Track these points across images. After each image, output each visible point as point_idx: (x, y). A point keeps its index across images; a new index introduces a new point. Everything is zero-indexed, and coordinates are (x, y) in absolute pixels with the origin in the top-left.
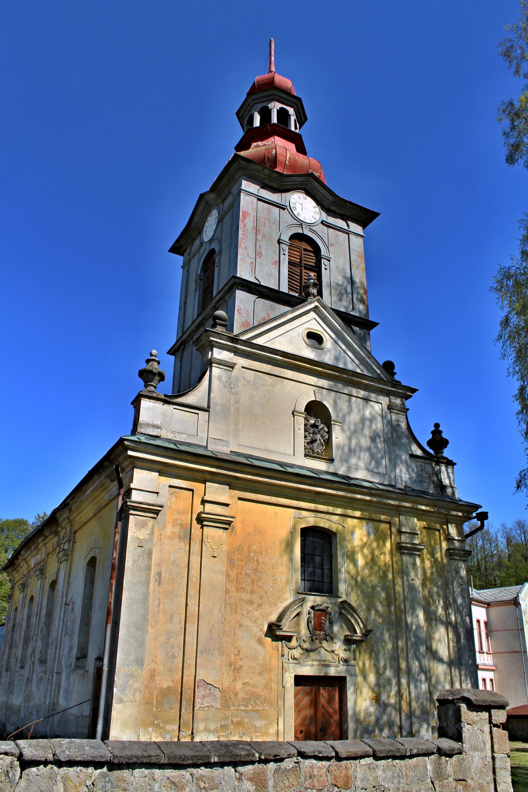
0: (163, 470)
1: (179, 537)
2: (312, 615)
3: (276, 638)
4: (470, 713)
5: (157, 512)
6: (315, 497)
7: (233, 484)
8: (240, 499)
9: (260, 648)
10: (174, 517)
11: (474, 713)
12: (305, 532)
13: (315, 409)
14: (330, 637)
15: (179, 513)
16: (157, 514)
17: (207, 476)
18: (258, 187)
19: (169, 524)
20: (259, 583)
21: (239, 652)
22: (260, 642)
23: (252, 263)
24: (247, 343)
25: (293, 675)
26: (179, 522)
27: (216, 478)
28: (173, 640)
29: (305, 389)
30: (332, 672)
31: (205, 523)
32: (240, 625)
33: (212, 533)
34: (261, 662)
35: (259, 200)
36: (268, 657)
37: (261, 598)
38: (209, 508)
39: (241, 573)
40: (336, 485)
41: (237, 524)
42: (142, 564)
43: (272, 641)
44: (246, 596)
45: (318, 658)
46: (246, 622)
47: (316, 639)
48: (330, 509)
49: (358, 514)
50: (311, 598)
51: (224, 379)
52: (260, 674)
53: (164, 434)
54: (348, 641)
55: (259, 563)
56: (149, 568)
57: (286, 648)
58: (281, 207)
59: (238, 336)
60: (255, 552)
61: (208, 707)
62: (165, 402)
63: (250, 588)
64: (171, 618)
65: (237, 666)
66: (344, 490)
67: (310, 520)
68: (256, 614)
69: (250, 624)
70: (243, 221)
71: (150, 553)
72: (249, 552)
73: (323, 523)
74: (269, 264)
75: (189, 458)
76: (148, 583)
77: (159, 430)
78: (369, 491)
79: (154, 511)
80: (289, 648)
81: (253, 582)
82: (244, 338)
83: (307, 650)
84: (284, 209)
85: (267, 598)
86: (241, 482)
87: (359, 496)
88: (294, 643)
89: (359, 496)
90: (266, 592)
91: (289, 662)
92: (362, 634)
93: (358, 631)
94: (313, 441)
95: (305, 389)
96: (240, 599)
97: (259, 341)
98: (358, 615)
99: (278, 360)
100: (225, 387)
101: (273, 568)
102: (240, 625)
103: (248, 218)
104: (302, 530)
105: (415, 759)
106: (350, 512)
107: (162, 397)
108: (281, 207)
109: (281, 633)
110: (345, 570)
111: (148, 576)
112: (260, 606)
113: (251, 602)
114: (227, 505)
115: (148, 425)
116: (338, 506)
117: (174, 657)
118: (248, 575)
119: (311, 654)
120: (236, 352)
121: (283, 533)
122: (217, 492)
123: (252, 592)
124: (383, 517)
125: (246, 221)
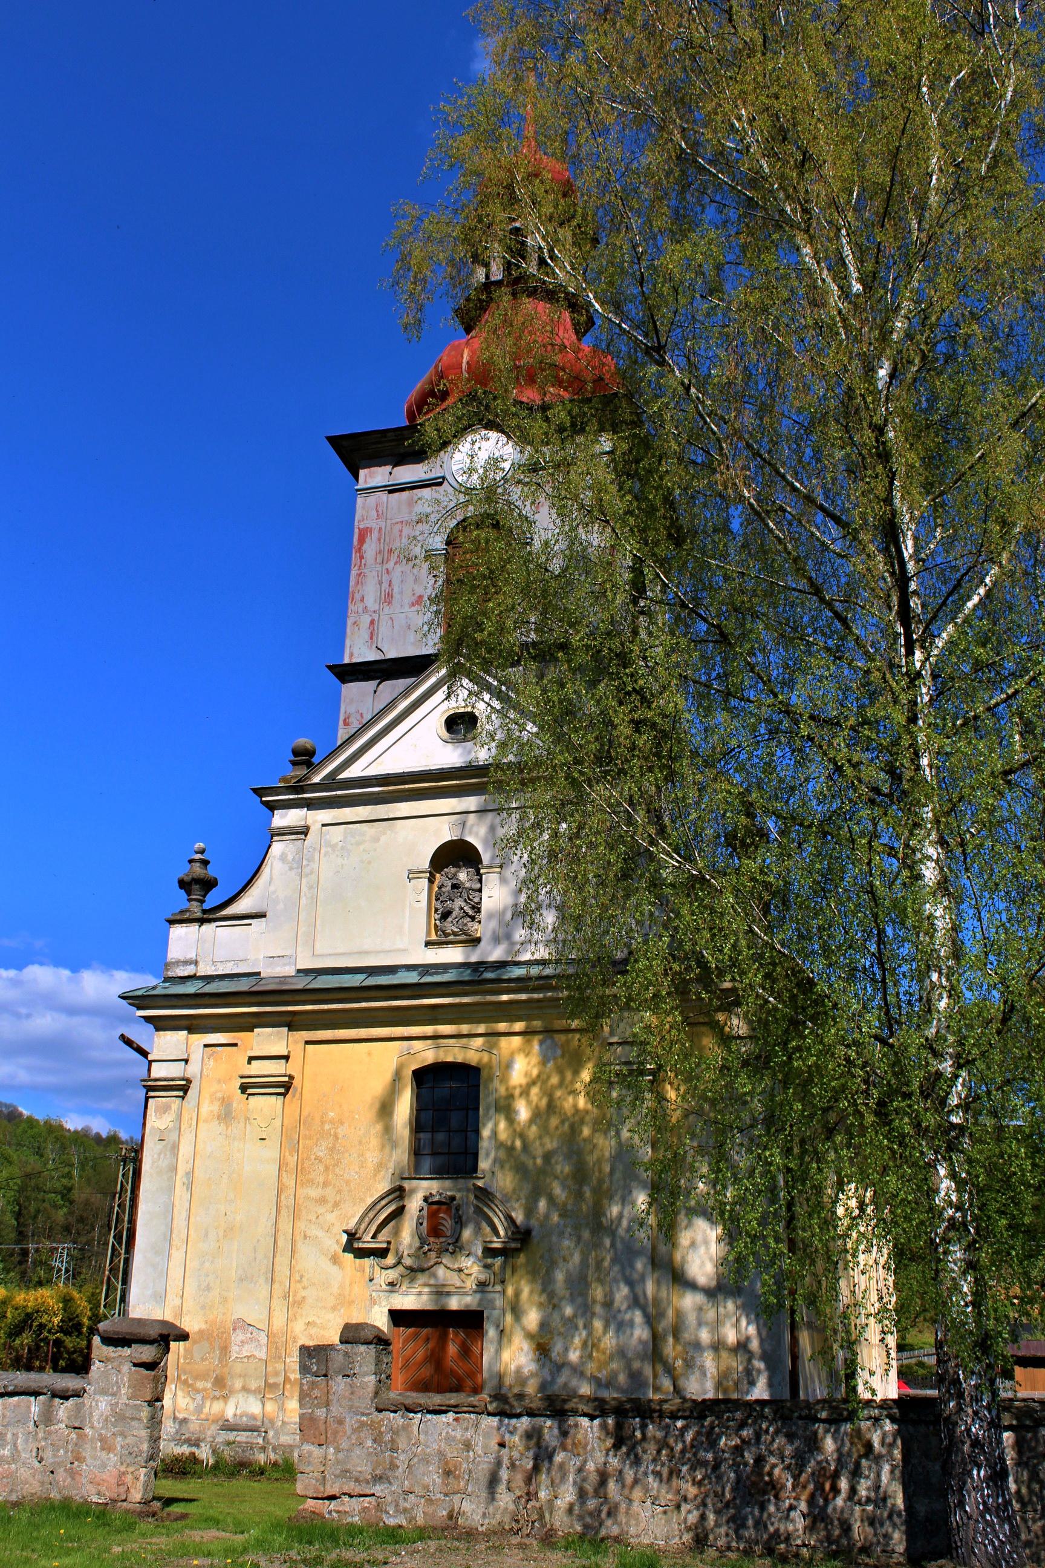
0: (192, 1026)
1: (219, 1117)
2: (425, 1213)
3: (361, 1253)
4: (104, 1348)
5: (185, 1089)
6: (433, 1015)
7: (293, 1023)
8: (307, 1042)
9: (334, 1270)
10: (213, 1090)
11: (111, 1349)
12: (420, 1075)
13: (455, 855)
14: (455, 1247)
15: (219, 1081)
16: (186, 1092)
17: (254, 1020)
18: (389, 468)
19: (204, 1100)
20: (337, 1170)
21: (302, 1277)
22: (335, 1260)
23: (372, 622)
24: (331, 782)
25: (386, 1310)
26: (219, 1095)
27: (264, 1020)
28: (207, 1265)
29: (431, 825)
30: (454, 1304)
31: (250, 1091)
32: (305, 1237)
33: (265, 1104)
34: (335, 1290)
35: (390, 492)
36: (347, 1283)
37: (339, 1192)
38: (258, 1067)
39: (308, 1158)
40: (453, 989)
41: (305, 1085)
42: (164, 1163)
44: (314, 1193)
46: (314, 1231)
48: (465, 1028)
49: (519, 1026)
50: (425, 1184)
51: (290, 857)
52: (334, 1309)
53: (204, 970)
54: (490, 1252)
55: (337, 1138)
56: (174, 1169)
57: (377, 1268)
58: (437, 483)
59: (309, 778)
60: (332, 1122)
61: (248, 1357)
62: (202, 921)
63: (322, 1179)
64: (206, 1235)
65: (298, 1298)
66: (480, 992)
67: (427, 1054)
68: (331, 1217)
69: (320, 1234)
70: (360, 550)
71: (175, 1148)
72: (323, 1123)
73: (454, 1054)
74: (407, 609)
75: (213, 1001)
76: (171, 1189)
77: (193, 966)
78: (522, 985)
79: (183, 1088)
81: (327, 1168)
82: (316, 779)
84: (440, 484)
85: (350, 1191)
86: (303, 1017)
87: (505, 998)
89: (505, 998)
90: (348, 1182)
94: (445, 915)
95: (431, 825)
96: (307, 1198)
97: (354, 771)
99: (379, 793)
100: (291, 869)
101: (360, 1143)
102: (305, 1237)
103: (368, 540)
104: (415, 1073)
105: (16, 1398)
106: (502, 1026)
107: (199, 915)
108: (437, 483)
109: (361, 1245)
110: (493, 1130)
111: (172, 1181)
112: (336, 1204)
113: (322, 1201)
114: (286, 1058)
115: (178, 963)
116: (479, 1021)
117: (208, 1288)
118: (319, 1160)
119: (419, 1275)
120: (310, 805)
121: (379, 1085)
122: (270, 1040)
123: (326, 1184)
124: (575, 1024)
125: (365, 547)
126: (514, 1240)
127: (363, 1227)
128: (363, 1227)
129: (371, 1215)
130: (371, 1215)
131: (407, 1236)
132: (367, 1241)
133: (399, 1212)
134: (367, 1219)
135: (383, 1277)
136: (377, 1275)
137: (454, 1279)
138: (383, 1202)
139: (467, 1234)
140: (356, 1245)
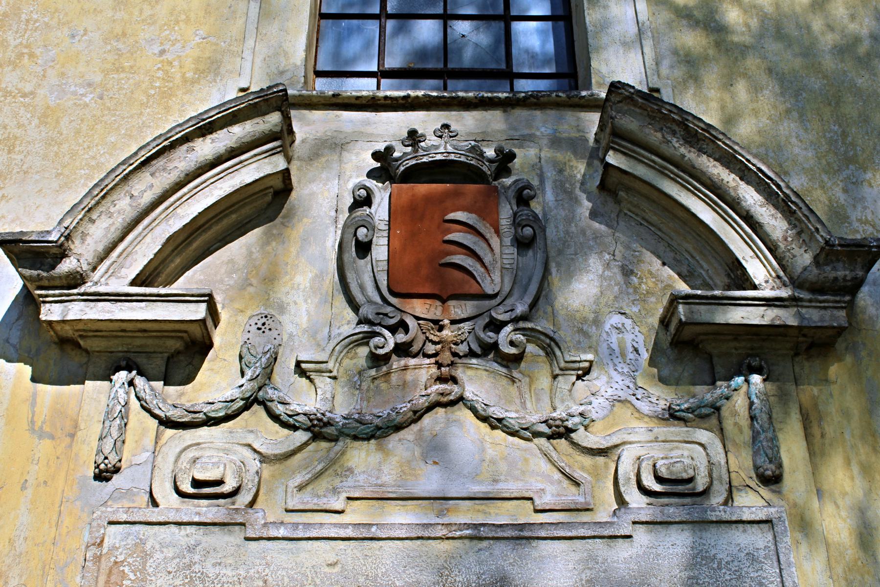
2: (380, 210)
3: (69, 356)
14: (520, 334)
43: (34, 380)
45: (429, 481)
47: (402, 350)
54: (693, 351)
57: (142, 424)
80: (167, 423)
83: (319, 429)
88: (217, 381)
91: (154, 515)
92: (795, 282)
93: (758, 270)
98: (730, 161)
126: (817, 289)
127: (99, 232)
128: (99, 232)
129: (147, 186)
130: (147, 186)
131: (294, 297)
132: (110, 295)
133: (267, 203)
134: (123, 206)
135: (158, 461)
136: (135, 454)
137: (536, 475)
138: (206, 148)
139: (583, 289)
140: (51, 312)
